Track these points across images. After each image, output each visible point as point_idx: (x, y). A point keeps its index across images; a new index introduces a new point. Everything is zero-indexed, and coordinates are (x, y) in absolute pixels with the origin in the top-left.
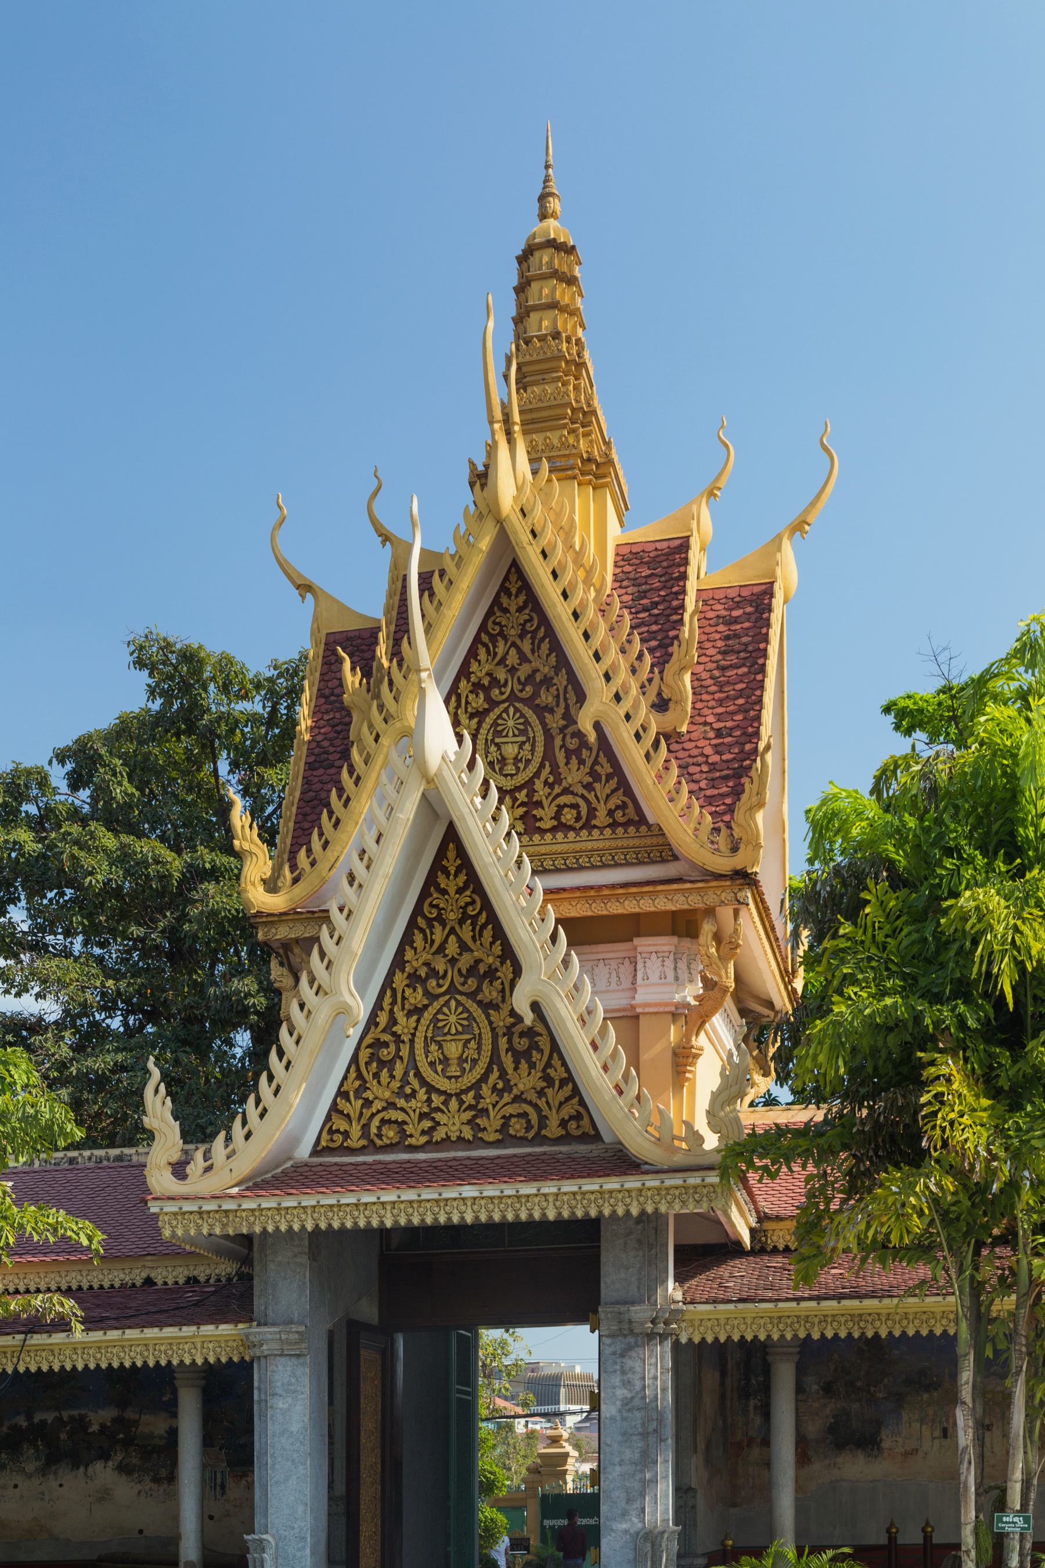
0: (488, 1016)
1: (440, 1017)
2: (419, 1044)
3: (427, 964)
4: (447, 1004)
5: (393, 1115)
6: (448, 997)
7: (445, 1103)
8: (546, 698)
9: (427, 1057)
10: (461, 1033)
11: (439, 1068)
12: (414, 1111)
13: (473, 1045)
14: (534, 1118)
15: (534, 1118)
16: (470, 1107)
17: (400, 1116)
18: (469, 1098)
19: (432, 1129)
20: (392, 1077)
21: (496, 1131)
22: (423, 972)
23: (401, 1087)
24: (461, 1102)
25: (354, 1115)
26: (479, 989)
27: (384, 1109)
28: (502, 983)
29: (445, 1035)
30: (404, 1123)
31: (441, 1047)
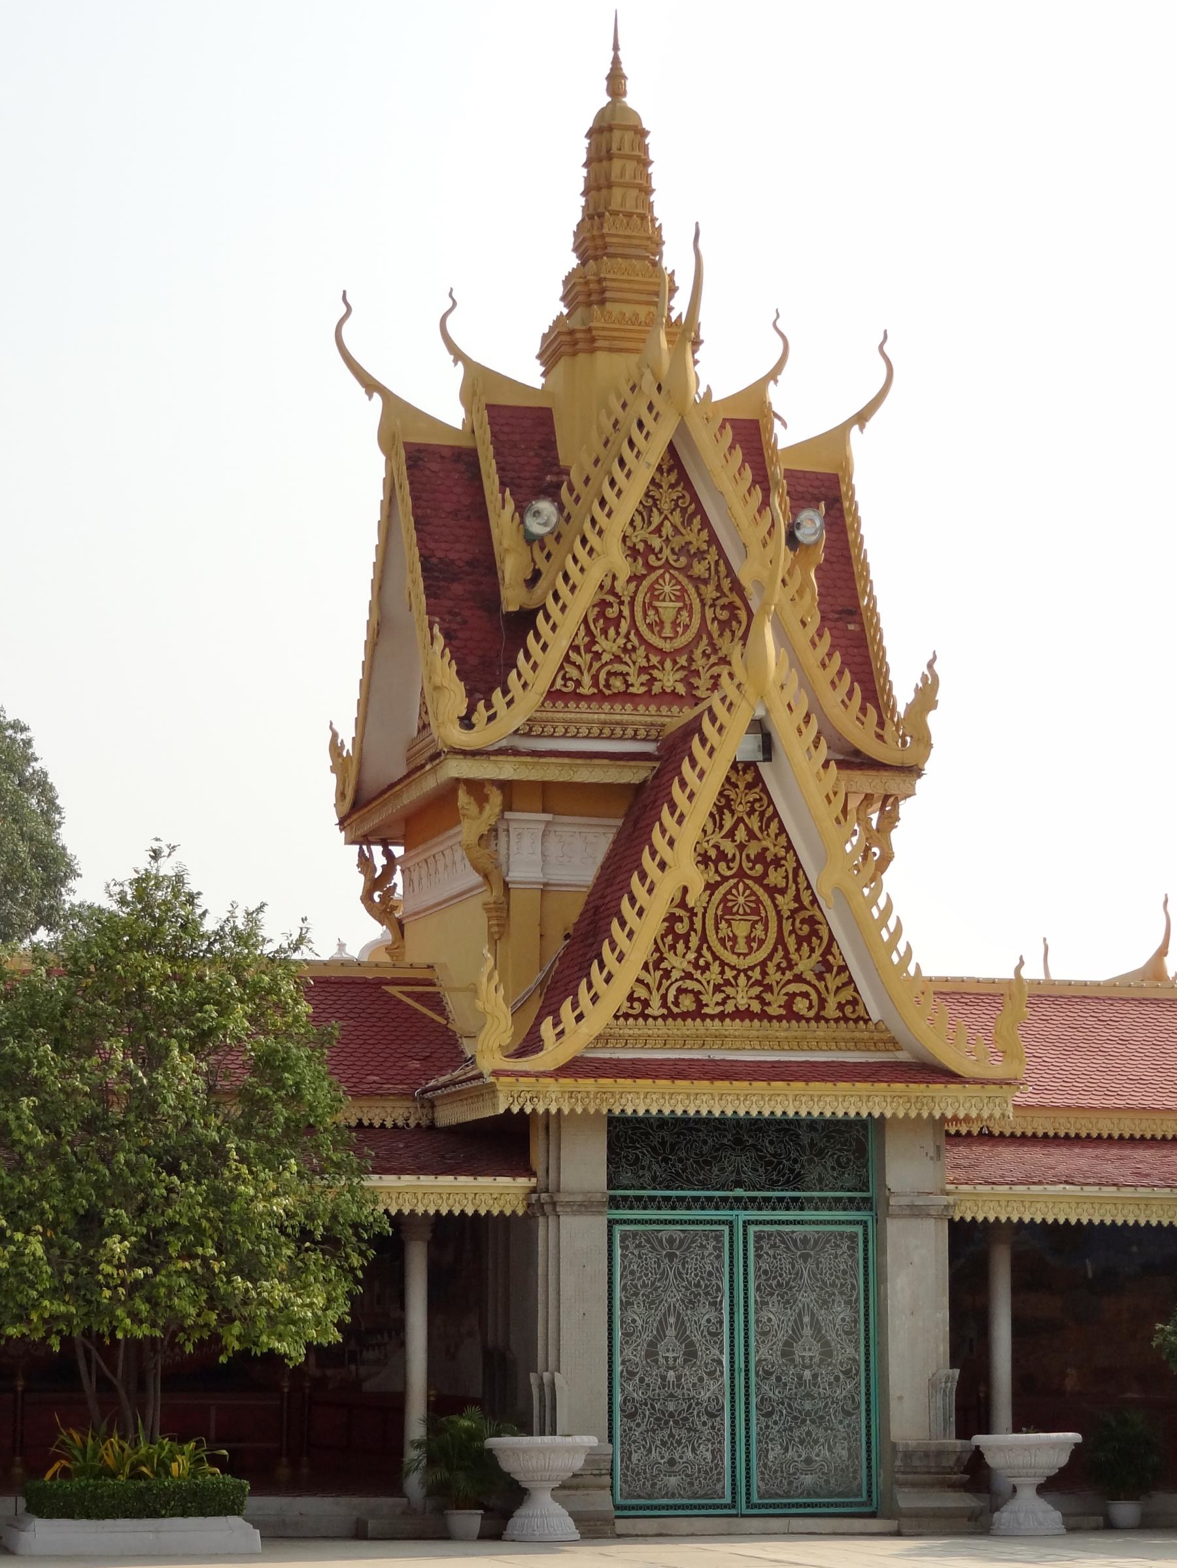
0: (773, 900)
1: (729, 897)
2: (710, 923)
3: (716, 847)
4: (736, 886)
5: (689, 984)
6: (735, 880)
7: (736, 978)
8: (699, 569)
9: (717, 933)
10: (749, 914)
11: (729, 944)
12: (708, 982)
13: (759, 927)
14: (814, 996)
15: (814, 996)
16: (758, 983)
17: (696, 987)
18: (756, 974)
19: (723, 1002)
20: (688, 948)
21: (780, 1006)
22: (713, 853)
23: (697, 959)
24: (749, 978)
25: (654, 986)
26: (765, 874)
27: (682, 978)
28: (786, 871)
29: (734, 914)
30: (700, 993)
31: (730, 925)
